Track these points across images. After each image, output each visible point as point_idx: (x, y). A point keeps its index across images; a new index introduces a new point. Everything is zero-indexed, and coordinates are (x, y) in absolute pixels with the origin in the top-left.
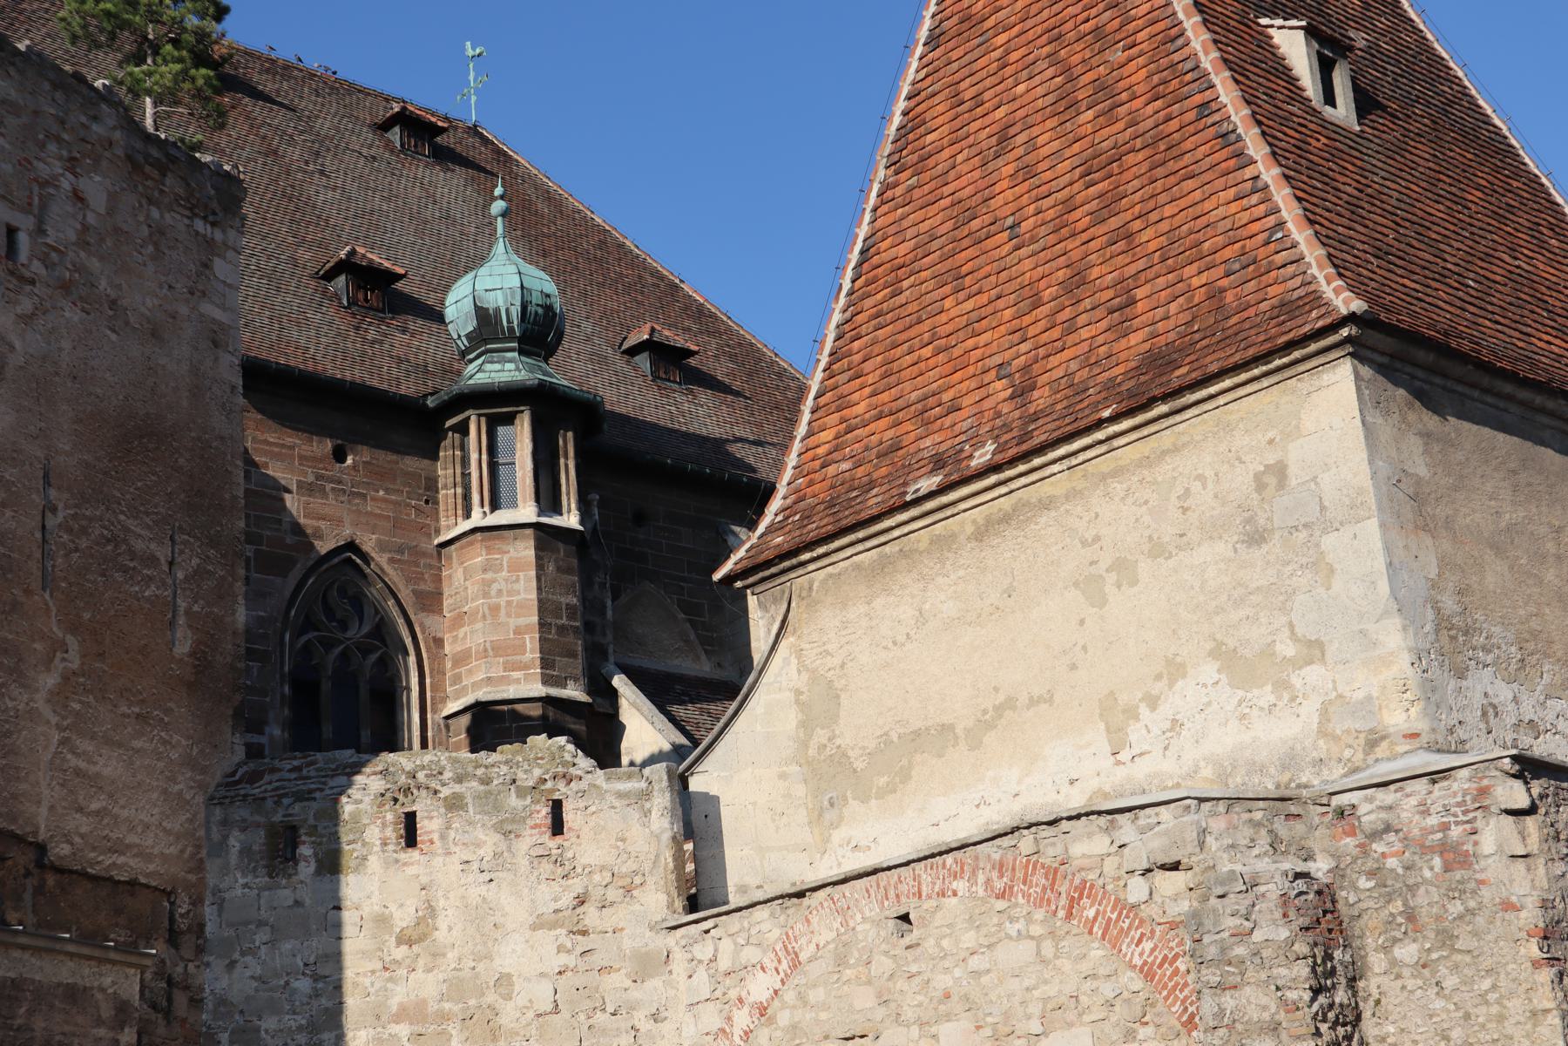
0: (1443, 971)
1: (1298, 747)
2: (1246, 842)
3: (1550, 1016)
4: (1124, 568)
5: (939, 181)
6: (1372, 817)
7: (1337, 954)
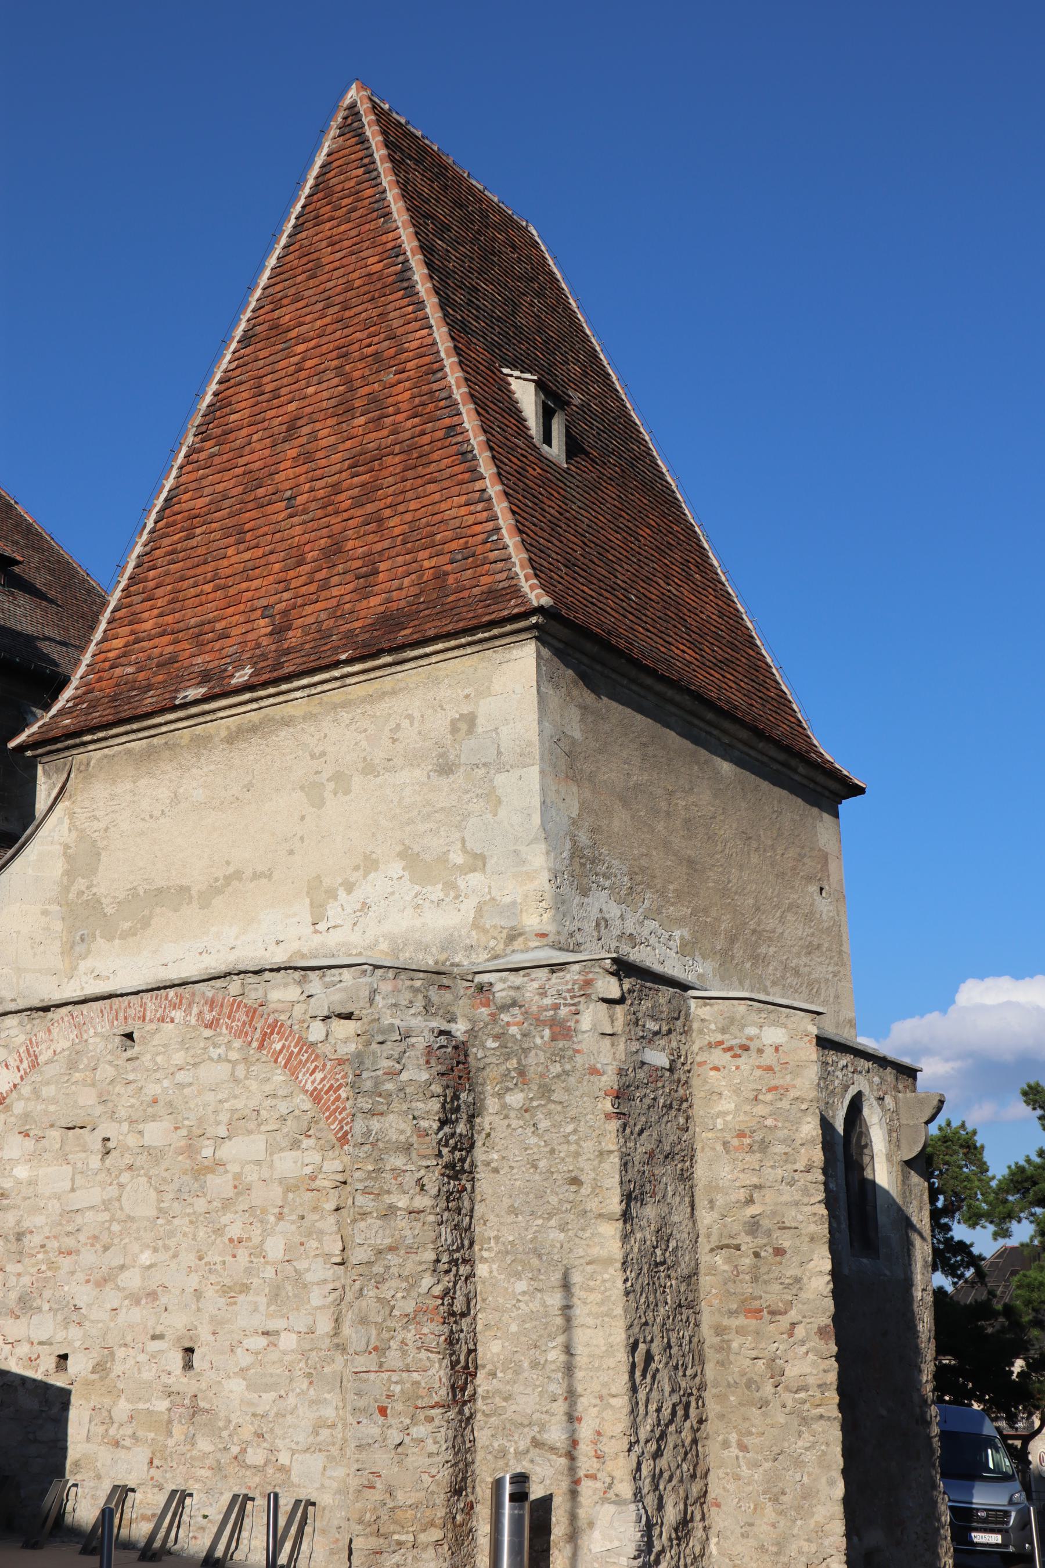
0: (540, 1116)
1: (456, 934)
2: (406, 1003)
3: (612, 1156)
5: (237, 453)
6: (504, 994)
7: (463, 1096)
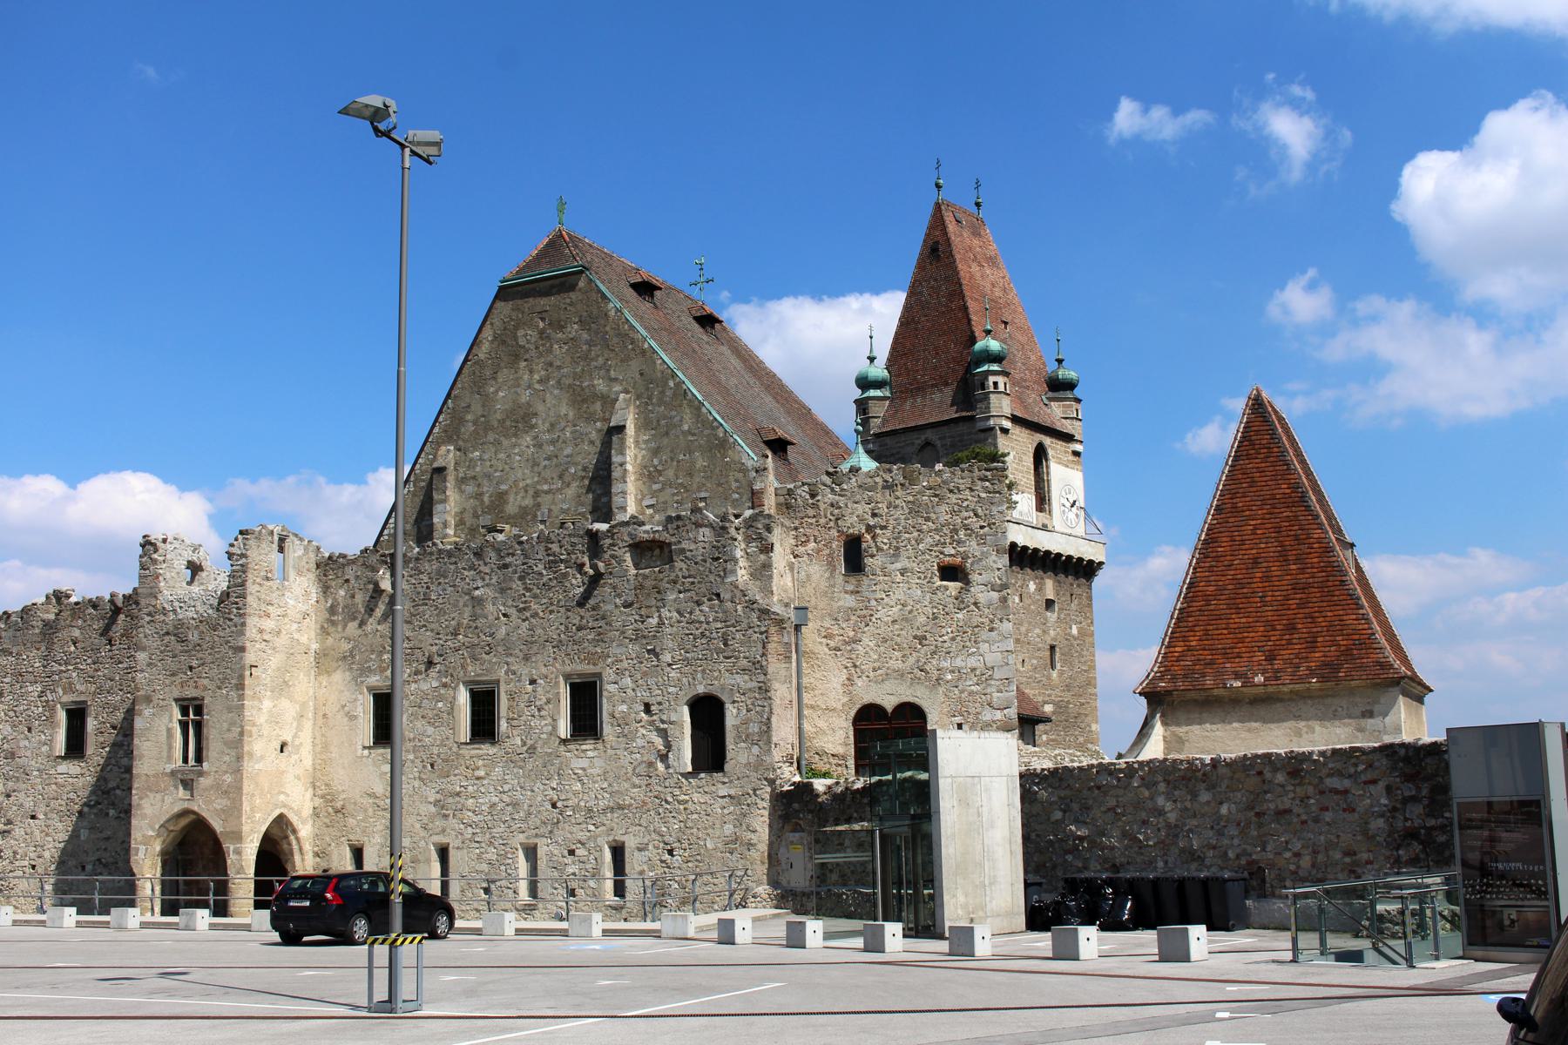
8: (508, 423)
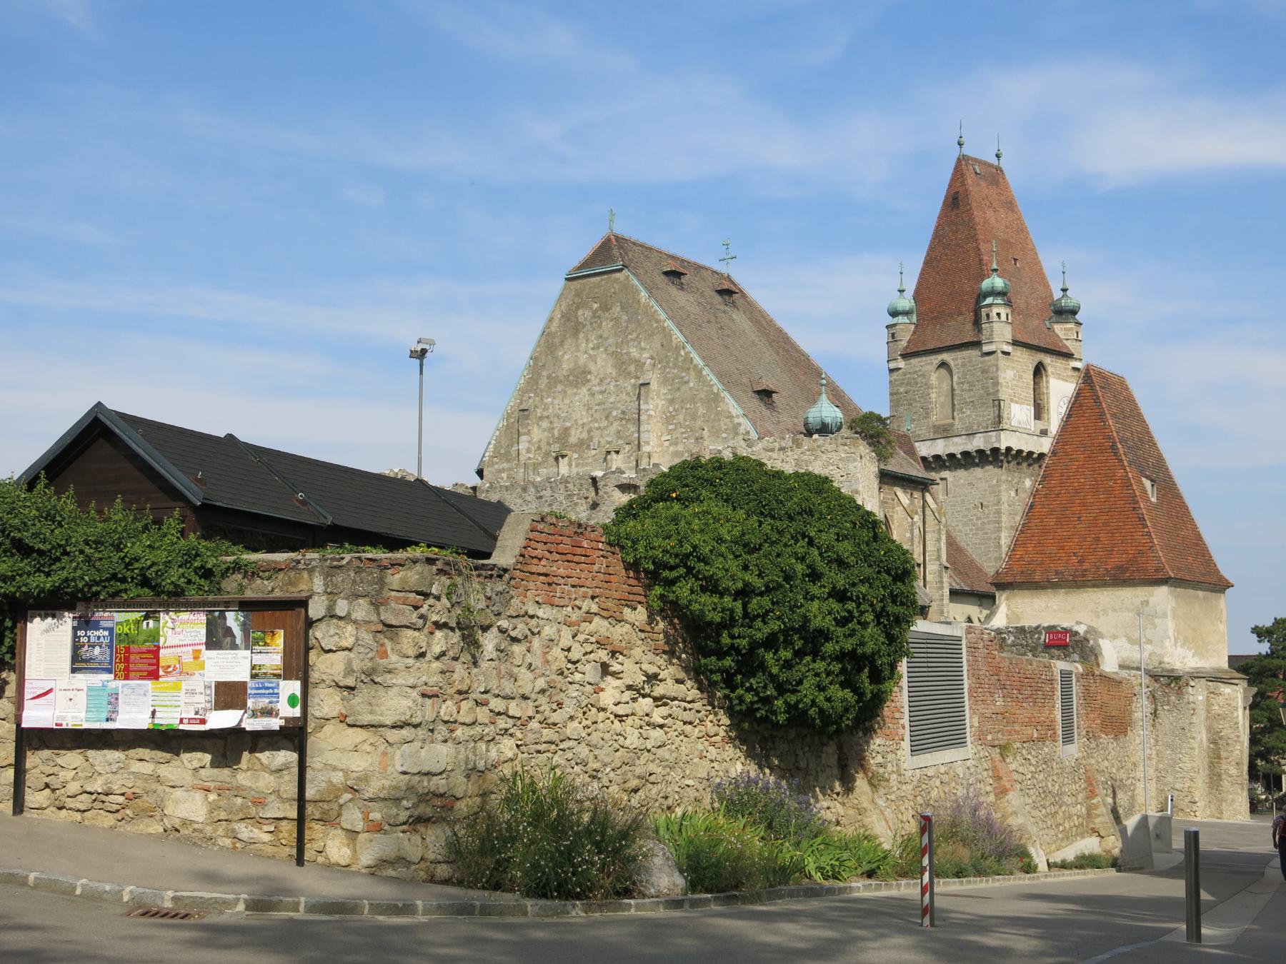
4: (1105, 612)
8: (571, 378)
